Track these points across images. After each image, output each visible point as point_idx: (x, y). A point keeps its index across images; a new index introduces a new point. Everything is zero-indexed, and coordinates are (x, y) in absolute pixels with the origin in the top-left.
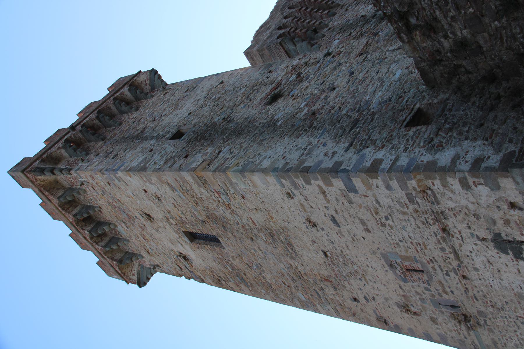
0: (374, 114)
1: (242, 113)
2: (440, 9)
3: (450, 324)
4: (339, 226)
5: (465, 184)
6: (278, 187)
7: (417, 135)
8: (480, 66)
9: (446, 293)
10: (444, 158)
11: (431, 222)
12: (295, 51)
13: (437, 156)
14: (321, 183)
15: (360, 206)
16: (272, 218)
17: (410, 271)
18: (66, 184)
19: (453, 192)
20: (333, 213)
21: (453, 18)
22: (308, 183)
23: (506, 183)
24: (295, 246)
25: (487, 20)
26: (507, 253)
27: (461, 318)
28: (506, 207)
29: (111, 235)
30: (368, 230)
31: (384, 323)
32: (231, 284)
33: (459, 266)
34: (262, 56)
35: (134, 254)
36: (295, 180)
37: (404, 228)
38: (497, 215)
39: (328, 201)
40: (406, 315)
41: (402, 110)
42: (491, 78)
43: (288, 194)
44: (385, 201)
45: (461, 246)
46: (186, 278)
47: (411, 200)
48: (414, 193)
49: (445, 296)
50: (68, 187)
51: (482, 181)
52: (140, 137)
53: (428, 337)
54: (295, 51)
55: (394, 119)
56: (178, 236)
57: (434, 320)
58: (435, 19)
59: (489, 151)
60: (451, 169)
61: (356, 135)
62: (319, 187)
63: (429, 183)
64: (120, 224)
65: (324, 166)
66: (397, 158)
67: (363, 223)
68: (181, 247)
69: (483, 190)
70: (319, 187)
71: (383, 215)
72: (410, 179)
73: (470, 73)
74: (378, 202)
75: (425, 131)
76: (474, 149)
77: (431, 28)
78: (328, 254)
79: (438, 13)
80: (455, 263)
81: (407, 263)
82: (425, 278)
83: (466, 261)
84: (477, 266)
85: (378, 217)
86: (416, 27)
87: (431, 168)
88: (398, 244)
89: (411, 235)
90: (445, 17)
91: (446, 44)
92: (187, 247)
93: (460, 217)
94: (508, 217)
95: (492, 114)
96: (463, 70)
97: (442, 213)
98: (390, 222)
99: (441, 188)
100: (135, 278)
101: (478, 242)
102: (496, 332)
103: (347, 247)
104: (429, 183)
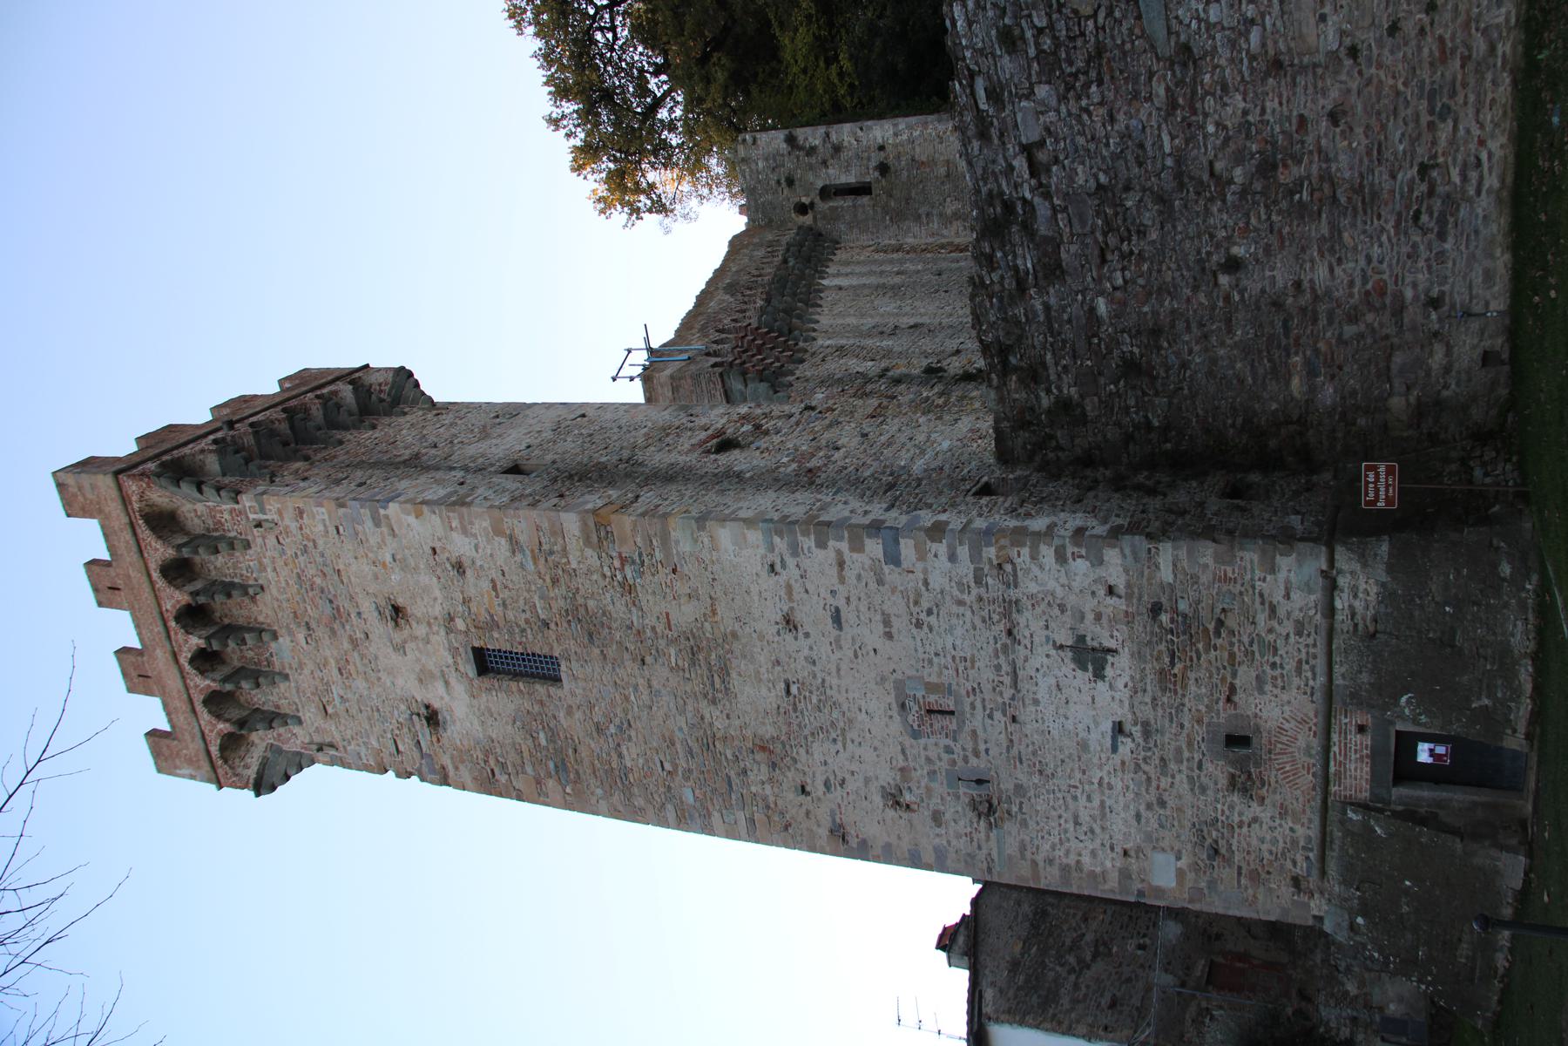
0: (919, 480)
1: (658, 458)
2: (1054, 354)
3: (962, 823)
4: (840, 628)
5: (1061, 557)
6: (762, 551)
8: (1077, 441)
9: (976, 754)
10: (1039, 524)
11: (996, 617)
12: (742, 393)
13: (1027, 523)
14: (844, 546)
15: (894, 590)
16: (714, 612)
17: (932, 712)
18: (195, 525)
19: (1041, 567)
20: (841, 603)
21: (1065, 367)
22: (822, 544)
23: (1112, 555)
24: (734, 675)
25: (1102, 381)
26: (1086, 670)
27: (984, 808)
28: (1102, 592)
29: (237, 664)
30: (889, 636)
32: (518, 783)
33: (1013, 698)
34: (675, 389)
35: (278, 714)
36: (800, 538)
37: (951, 630)
38: (1089, 605)
39: (842, 580)
40: (890, 813)
41: (964, 480)
42: (1087, 461)
43: (772, 566)
44: (937, 581)
45: (1026, 660)
46: (399, 775)
47: (978, 581)
48: (986, 569)
49: (973, 761)
50: (199, 531)
51: (1083, 552)
52: (414, 464)
53: (915, 861)
54: (742, 393)
56: (450, 661)
57: (937, 818)
58: (1044, 364)
59: (1091, 522)
61: (896, 499)
62: (839, 553)
63: (1013, 553)
64: (291, 633)
65: (853, 521)
66: (970, 522)
67: (887, 622)
68: (440, 687)
69: (1081, 566)
70: (839, 553)
71: (925, 605)
72: (988, 545)
73: (1063, 449)
74: (926, 583)
76: (1077, 520)
77: (1034, 375)
78: (794, 689)
79: (1049, 356)
80: (1008, 693)
81: (932, 698)
82: (954, 726)
83: (1024, 686)
84: (1039, 696)
85: (915, 610)
86: (1016, 369)
88: (930, 662)
89: (958, 643)
90: (1056, 364)
91: (1046, 402)
92: (459, 688)
93: (1038, 610)
94: (1102, 609)
95: (1091, 494)
96: (1054, 443)
97: (1017, 602)
98: (932, 619)
99: (1028, 559)
100: (252, 773)
101: (1053, 652)
102: (1032, 824)
103: (838, 670)
104: (1013, 553)
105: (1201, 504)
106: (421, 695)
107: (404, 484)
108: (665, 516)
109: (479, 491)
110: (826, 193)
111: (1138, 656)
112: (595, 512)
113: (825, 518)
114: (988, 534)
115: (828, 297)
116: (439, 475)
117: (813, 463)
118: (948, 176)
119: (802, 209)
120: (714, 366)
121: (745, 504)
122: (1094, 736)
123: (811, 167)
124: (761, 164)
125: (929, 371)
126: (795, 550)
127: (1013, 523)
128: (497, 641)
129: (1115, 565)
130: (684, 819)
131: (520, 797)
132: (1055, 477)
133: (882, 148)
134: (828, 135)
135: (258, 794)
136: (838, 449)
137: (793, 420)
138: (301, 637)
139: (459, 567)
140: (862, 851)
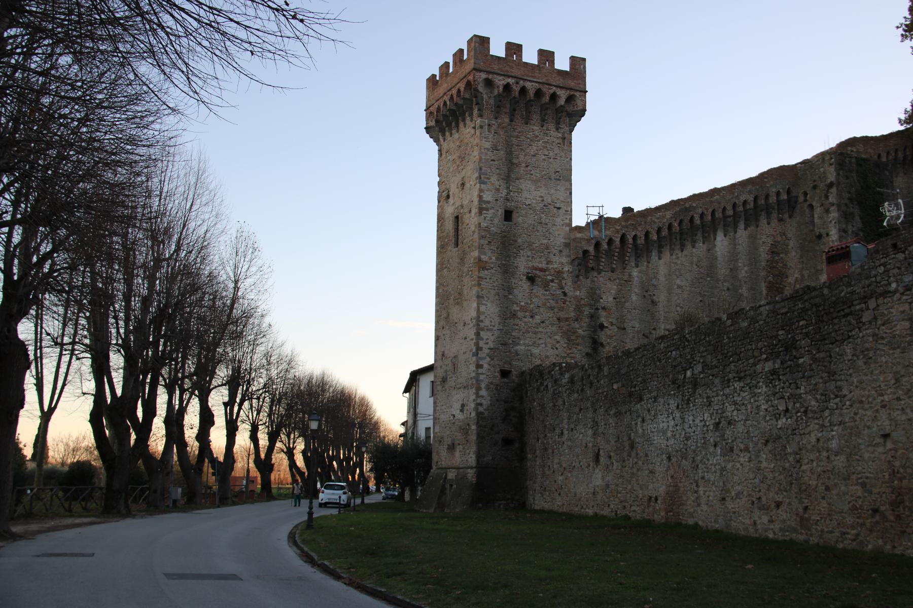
0: (510, 351)
7: (495, 377)
10: (483, 392)
52: (510, 171)
55: (505, 363)
60: (478, 396)
66: (483, 374)
75: (497, 379)
76: (486, 402)
87: (479, 389)
107: (494, 179)
108: (479, 285)
109: (492, 211)
110: (811, 207)
111: (463, 421)
112: (480, 260)
113: (482, 333)
114: (478, 381)
115: (701, 248)
117: (520, 314)
118: (817, 270)
119: (805, 194)
120: (585, 252)
121: (489, 305)
123: (820, 198)
124: (822, 170)
125: (602, 327)
127: (483, 386)
129: (473, 414)
133: (828, 235)
134: (833, 205)
136: (532, 317)
139: (470, 212)
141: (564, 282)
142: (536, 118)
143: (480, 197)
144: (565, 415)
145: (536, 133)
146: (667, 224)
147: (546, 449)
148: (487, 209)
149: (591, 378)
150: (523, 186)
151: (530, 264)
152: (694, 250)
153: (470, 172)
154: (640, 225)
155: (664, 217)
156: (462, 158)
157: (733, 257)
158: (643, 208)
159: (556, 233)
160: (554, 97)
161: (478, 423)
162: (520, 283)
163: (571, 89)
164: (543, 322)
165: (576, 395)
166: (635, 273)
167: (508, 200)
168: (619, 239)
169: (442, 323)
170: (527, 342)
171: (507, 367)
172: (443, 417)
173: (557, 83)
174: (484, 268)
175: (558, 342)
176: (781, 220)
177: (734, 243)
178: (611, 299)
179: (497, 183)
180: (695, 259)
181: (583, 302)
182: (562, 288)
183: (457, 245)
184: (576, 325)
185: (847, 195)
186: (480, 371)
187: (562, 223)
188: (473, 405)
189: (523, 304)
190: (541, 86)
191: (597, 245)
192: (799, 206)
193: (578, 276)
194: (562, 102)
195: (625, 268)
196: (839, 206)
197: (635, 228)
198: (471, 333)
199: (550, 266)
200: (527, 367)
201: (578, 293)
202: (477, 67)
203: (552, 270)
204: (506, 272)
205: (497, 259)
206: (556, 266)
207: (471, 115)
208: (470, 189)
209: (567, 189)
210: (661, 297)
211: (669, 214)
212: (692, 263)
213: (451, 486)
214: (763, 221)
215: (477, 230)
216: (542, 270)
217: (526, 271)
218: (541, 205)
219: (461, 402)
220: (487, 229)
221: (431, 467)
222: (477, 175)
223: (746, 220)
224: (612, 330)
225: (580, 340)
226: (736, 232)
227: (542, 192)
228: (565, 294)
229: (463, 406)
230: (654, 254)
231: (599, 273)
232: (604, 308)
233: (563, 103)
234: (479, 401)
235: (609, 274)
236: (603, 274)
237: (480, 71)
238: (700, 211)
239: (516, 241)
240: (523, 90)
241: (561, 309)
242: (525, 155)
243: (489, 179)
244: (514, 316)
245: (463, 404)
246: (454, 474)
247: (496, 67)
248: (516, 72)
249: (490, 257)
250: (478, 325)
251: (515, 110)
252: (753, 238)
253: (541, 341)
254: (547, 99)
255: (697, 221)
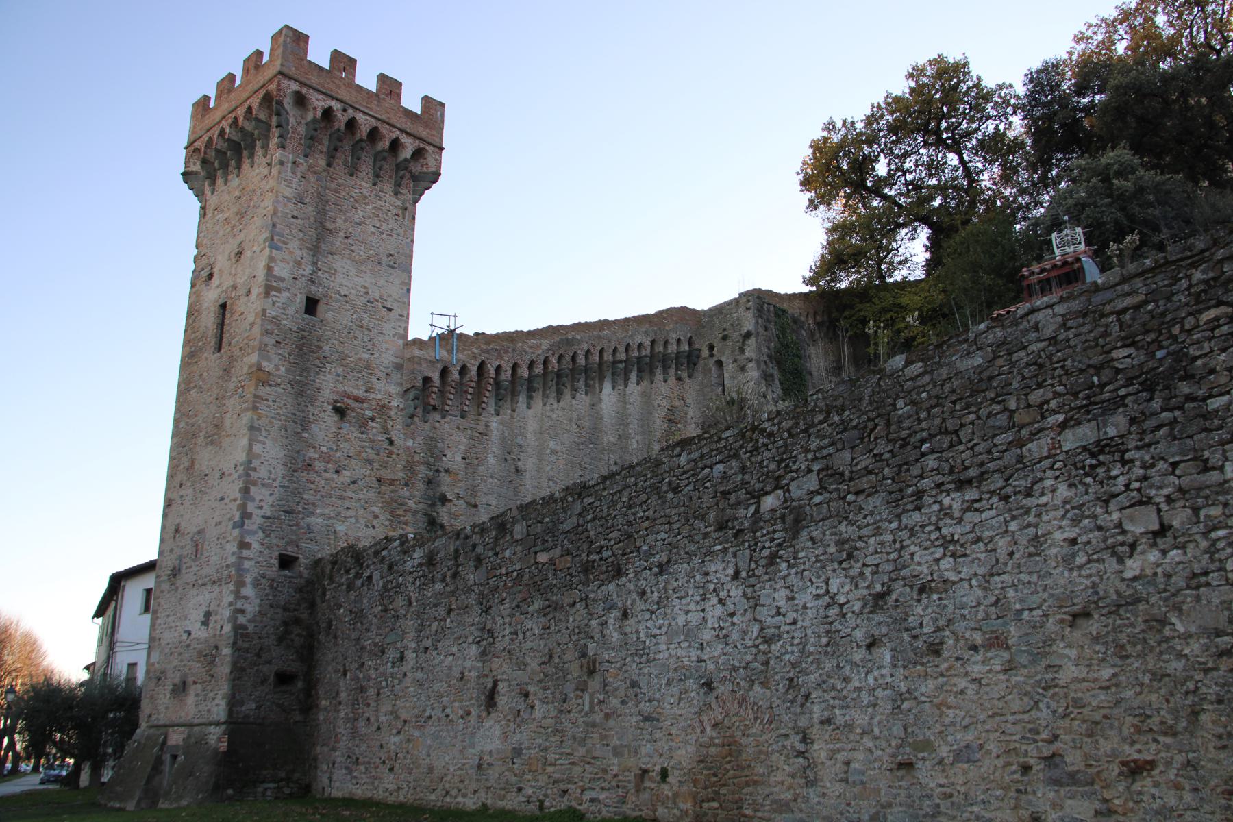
0: (297, 525)
5: (231, 604)
7: (270, 566)
10: (248, 591)
14: (238, 502)
31: (168, 503)
52: (320, 238)
55: (288, 544)
59: (249, 616)
60: (238, 595)
75: (274, 571)
76: (251, 608)
80: (200, 582)
95: (279, 610)
105: (269, 662)
106: (216, 270)
107: (294, 245)
108: (255, 408)
110: (720, 364)
113: (253, 489)
114: (240, 570)
115: (583, 400)
116: (308, 258)
117: (318, 465)
119: (711, 347)
120: (427, 380)
121: (269, 443)
122: (187, 622)
125: (444, 500)
126: (239, 477)
127: (248, 579)
128: (228, 315)
129: (228, 628)
130: (177, 422)
131: (186, 331)
132: (300, 590)
134: (751, 361)
135: (183, 174)
136: (337, 472)
137: (382, 437)
138: (237, 194)
140: (165, 516)
141: (390, 422)
142: (366, 169)
143: (269, 269)
144: (410, 625)
145: (364, 191)
146: (542, 358)
147: (362, 689)
148: (278, 290)
149: (479, 550)
150: (337, 266)
151: (341, 388)
152: (574, 402)
153: (255, 233)
154: (507, 352)
155: (539, 347)
156: (241, 215)
157: (623, 422)
158: (513, 330)
159: (384, 346)
160: (395, 145)
161: (235, 643)
162: (322, 415)
163: (421, 139)
164: (354, 482)
165: (439, 586)
166: (494, 423)
167: (313, 282)
168: (476, 368)
169: (180, 477)
170: (327, 512)
171: (291, 551)
172: (168, 637)
173: (403, 126)
174: (265, 383)
175: (376, 517)
176: (679, 379)
177: (623, 401)
178: (458, 458)
179: (298, 253)
180: (575, 415)
181: (417, 458)
182: (387, 432)
183: (219, 349)
184: (405, 492)
185: (766, 351)
186: (245, 553)
187: (393, 332)
188: (227, 613)
189: (323, 448)
190: (379, 124)
191: (444, 372)
192: (701, 363)
193: (412, 417)
194: (407, 153)
195: (480, 415)
196: (758, 362)
197: (499, 356)
198: (233, 489)
199: (371, 396)
200: (325, 552)
201: (410, 443)
202: (285, 70)
203: (374, 403)
204: (300, 394)
205: (288, 371)
206: (379, 397)
207: (265, 147)
208: (252, 258)
209: (403, 283)
210: (529, 464)
211: (545, 344)
212: (570, 420)
213: (175, 757)
214: (659, 377)
215: (258, 321)
216: (357, 399)
217: (333, 397)
218: (364, 300)
219: (204, 609)
220: (276, 321)
221: (136, 725)
222: (266, 235)
223: (640, 370)
224: (458, 507)
225: (409, 517)
226: (626, 386)
227: (367, 280)
228: (391, 442)
229: (208, 614)
230: (522, 399)
231: (443, 417)
232: (447, 471)
233: (408, 156)
234: (239, 605)
235: (458, 420)
236: (448, 418)
237: (290, 78)
238: (585, 347)
239: (321, 348)
240: (351, 124)
241: (384, 465)
242: (345, 221)
243: (286, 243)
244: (309, 466)
245: (210, 612)
246: (182, 736)
247: (314, 80)
248: (343, 94)
249: (276, 365)
250: (248, 475)
251: (336, 150)
252: (646, 395)
253: (348, 513)
254: (385, 144)
255: (581, 361)
